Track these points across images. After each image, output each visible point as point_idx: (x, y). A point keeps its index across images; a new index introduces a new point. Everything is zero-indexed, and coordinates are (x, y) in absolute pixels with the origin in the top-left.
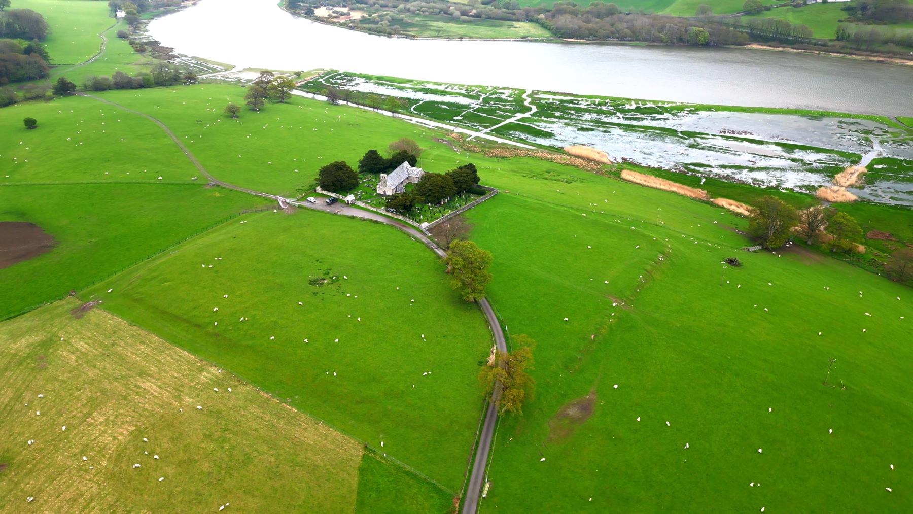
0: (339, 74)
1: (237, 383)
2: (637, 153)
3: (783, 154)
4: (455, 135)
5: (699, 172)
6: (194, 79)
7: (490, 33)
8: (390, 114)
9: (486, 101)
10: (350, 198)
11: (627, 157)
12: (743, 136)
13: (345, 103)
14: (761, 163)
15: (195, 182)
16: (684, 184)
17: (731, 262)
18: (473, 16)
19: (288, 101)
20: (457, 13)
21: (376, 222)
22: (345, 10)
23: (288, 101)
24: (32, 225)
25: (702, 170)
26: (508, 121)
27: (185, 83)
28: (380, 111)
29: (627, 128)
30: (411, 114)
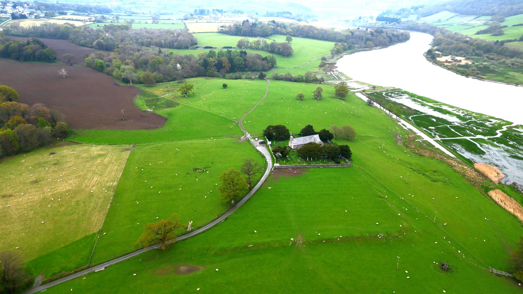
9: (468, 124)
13: (378, 106)
30: (408, 121)
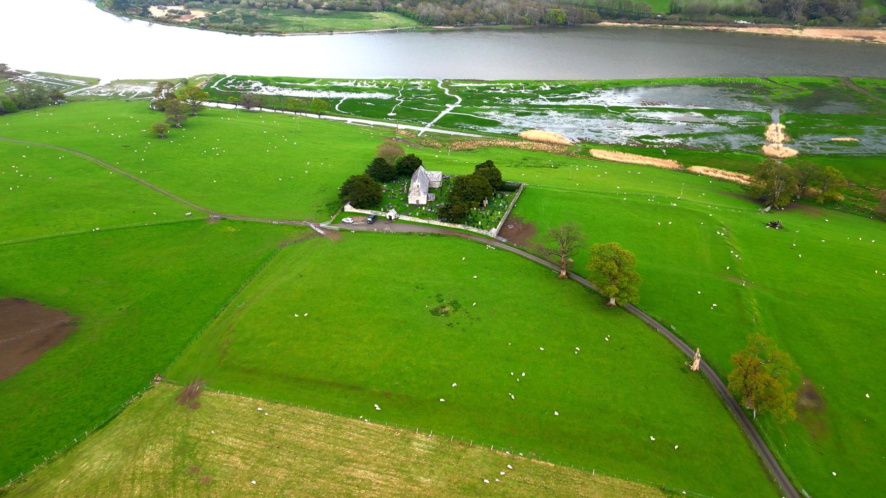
0: (230, 79)
1: (462, 447)
2: (586, 132)
3: (707, 119)
4: (403, 132)
6: (62, 97)
7: (356, 25)
8: (317, 116)
10: (392, 213)
11: (583, 137)
12: (666, 106)
13: (258, 109)
14: (698, 130)
15: (191, 218)
16: (644, 155)
17: (774, 225)
18: (324, 9)
19: (201, 112)
20: (309, 7)
21: (410, 234)
22: (181, 8)
23: (201, 112)
24: (21, 301)
26: (443, 113)
27: (53, 104)
28: (308, 115)
29: (560, 109)
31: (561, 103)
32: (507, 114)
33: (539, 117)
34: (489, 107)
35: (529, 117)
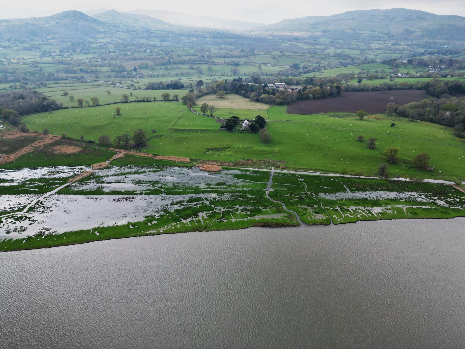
5: (156, 168)
25: (154, 169)
29: (197, 190)
31: (193, 196)
32: (231, 183)
33: (211, 183)
34: (245, 189)
35: (217, 182)
